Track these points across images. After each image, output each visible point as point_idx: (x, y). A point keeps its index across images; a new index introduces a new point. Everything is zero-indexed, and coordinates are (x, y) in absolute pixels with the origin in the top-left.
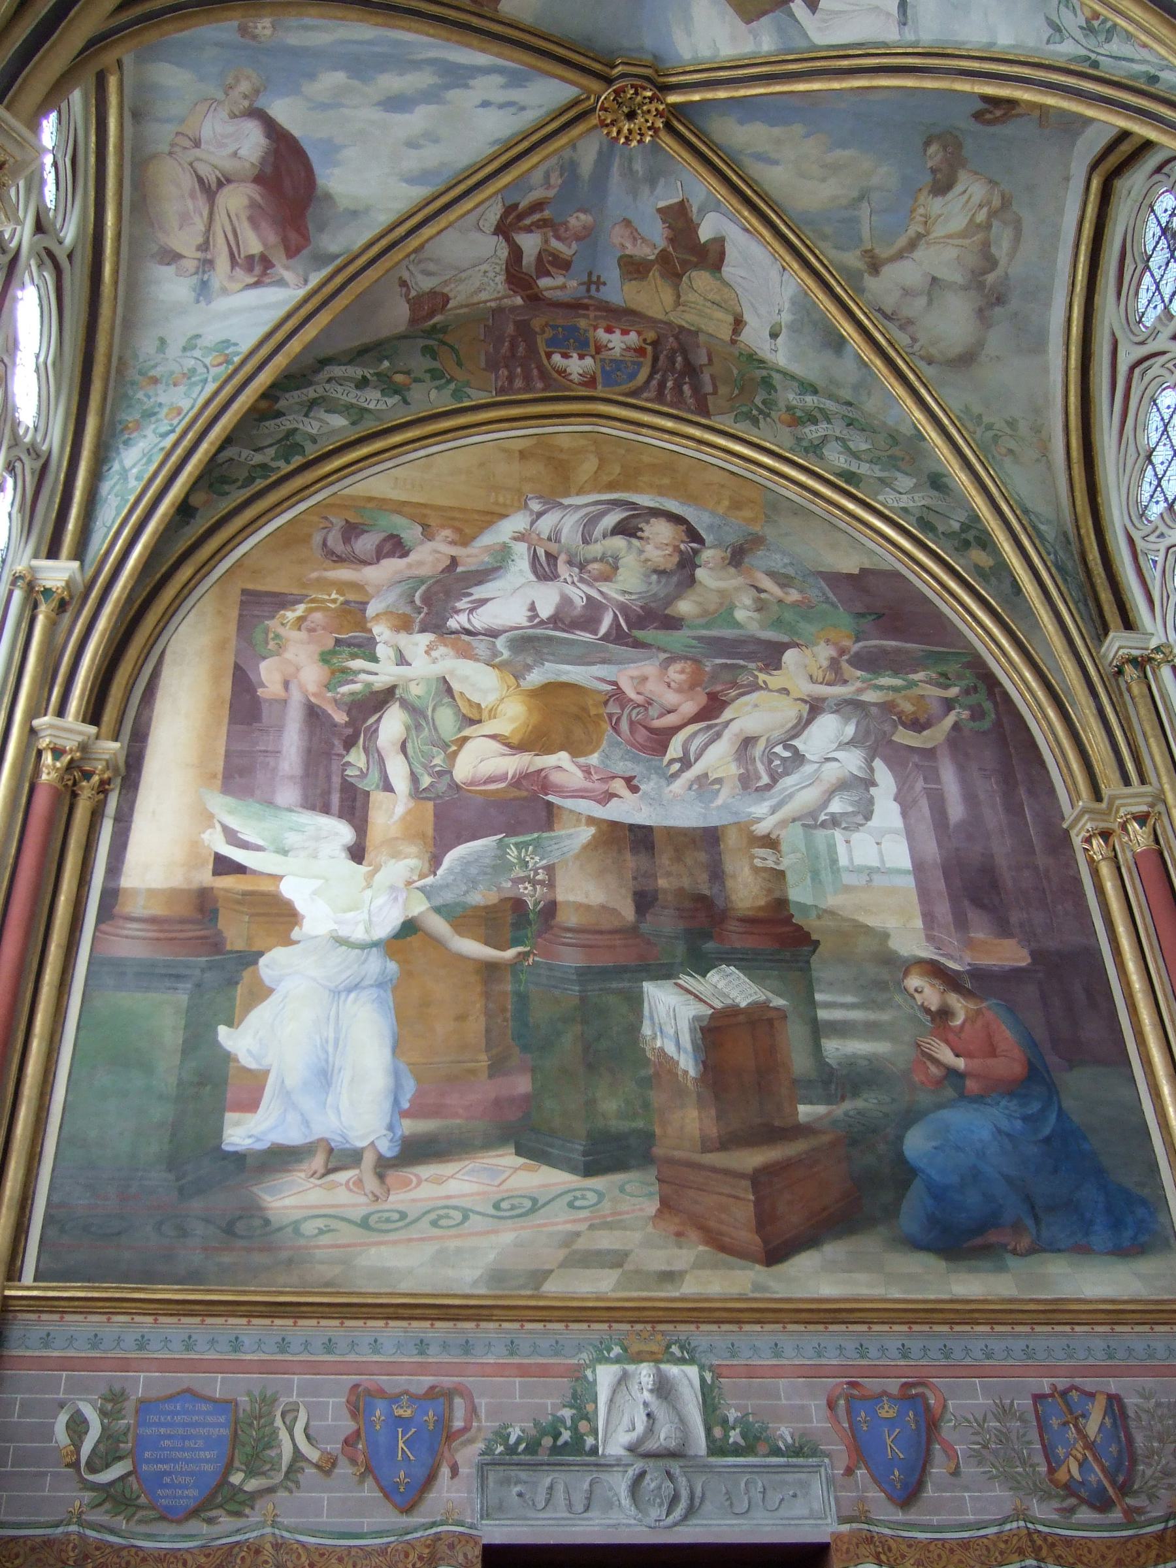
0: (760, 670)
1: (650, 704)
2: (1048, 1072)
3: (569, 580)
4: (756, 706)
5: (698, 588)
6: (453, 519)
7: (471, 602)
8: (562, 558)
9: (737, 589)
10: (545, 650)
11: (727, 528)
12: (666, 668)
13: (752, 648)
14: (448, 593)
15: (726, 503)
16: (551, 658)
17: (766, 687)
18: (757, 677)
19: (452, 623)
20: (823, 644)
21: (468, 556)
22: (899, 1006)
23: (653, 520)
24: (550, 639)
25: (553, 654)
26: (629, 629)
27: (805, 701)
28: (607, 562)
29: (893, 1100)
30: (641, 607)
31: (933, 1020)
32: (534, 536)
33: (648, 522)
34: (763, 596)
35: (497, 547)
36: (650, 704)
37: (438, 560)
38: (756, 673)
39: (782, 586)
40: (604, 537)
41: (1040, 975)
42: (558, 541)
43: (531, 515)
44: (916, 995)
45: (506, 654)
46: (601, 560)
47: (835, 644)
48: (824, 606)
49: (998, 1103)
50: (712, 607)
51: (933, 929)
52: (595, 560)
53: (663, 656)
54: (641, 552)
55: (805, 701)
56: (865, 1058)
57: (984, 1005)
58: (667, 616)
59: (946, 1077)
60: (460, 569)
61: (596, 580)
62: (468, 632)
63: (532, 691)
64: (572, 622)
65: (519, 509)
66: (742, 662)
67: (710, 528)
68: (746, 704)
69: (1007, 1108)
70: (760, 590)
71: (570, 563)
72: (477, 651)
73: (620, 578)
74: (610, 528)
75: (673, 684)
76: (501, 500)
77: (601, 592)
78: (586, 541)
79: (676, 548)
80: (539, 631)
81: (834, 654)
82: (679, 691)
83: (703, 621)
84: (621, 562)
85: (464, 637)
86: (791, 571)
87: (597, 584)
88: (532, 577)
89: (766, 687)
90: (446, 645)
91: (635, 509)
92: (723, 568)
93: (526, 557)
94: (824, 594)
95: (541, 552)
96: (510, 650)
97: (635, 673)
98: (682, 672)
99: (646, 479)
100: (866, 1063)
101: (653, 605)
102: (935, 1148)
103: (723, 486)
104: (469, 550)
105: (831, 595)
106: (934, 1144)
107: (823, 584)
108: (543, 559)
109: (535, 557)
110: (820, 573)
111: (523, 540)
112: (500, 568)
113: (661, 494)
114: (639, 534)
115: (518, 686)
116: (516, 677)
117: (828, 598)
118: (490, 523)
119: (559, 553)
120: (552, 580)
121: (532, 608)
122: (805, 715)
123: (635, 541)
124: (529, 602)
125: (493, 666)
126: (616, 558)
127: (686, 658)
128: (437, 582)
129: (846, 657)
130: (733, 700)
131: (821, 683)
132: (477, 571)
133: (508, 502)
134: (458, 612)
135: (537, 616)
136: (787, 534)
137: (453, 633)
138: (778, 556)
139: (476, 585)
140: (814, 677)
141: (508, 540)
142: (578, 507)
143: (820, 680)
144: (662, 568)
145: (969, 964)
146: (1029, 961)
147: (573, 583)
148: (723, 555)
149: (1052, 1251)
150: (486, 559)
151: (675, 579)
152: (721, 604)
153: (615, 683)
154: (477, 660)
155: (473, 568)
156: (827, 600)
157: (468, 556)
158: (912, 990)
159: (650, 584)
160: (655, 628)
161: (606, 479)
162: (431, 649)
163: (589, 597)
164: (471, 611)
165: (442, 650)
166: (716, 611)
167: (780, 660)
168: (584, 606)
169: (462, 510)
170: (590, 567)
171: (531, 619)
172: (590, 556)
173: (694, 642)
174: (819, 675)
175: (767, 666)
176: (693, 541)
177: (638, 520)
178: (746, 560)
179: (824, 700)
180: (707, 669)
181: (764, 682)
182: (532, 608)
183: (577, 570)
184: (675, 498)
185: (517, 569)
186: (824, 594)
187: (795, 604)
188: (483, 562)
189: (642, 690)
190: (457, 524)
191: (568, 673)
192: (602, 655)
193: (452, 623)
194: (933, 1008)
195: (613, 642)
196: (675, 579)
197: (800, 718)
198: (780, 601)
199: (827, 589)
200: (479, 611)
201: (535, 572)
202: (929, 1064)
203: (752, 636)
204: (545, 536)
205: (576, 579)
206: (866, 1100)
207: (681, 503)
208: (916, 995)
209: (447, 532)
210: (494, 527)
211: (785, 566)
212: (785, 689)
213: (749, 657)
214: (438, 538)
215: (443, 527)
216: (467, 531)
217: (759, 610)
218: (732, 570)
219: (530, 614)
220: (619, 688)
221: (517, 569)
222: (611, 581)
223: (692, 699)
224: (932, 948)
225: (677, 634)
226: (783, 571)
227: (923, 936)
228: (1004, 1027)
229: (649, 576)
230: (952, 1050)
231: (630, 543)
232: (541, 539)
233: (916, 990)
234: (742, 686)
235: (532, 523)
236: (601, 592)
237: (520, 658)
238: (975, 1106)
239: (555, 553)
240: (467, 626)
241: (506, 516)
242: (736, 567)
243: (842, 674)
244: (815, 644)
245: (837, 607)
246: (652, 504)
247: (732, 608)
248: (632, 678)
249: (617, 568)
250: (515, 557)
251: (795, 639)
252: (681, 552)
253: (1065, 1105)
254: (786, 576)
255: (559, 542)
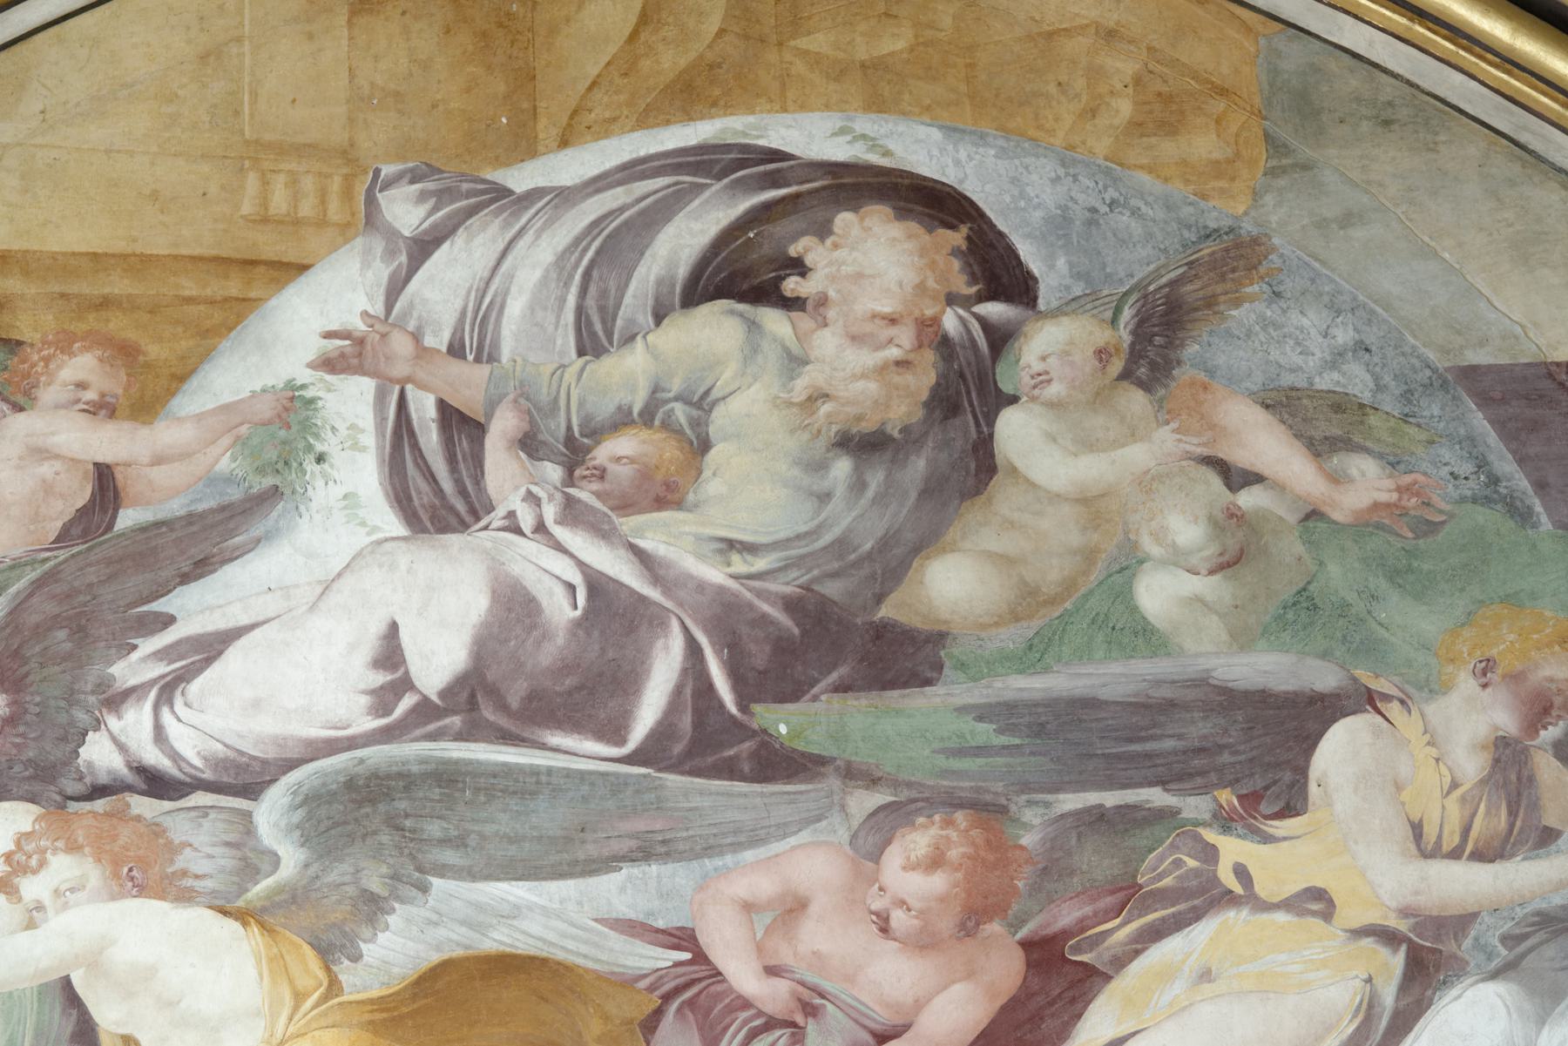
0: (1225, 821)
1: (810, 1010)
3: (526, 520)
4: (1206, 976)
5: (1004, 498)
6: (105, 303)
7: (162, 655)
8: (503, 426)
9: (1147, 482)
10: (434, 829)
11: (1123, 219)
12: (876, 856)
13: (1200, 729)
14: (81, 630)
15: (1124, 108)
16: (450, 856)
17: (1246, 896)
18: (1210, 854)
19: (99, 755)
20: (1466, 683)
21: (158, 460)
23: (844, 220)
24: (448, 777)
25: (459, 842)
26: (744, 708)
27: (1389, 937)
28: (666, 426)
30: (791, 605)
32: (401, 344)
33: (823, 231)
34: (1248, 499)
35: (266, 409)
36: (810, 1010)
37: (47, 488)
38: (1210, 836)
39: (1319, 448)
40: (659, 318)
42: (486, 354)
43: (390, 253)
45: (292, 859)
46: (647, 417)
47: (1515, 678)
48: (1483, 516)
50: (1052, 573)
52: (622, 421)
53: (864, 802)
54: (795, 362)
55: (1389, 937)
58: (883, 631)
60: (127, 519)
61: (626, 506)
62: (156, 784)
63: (380, 1003)
64: (532, 696)
65: (346, 232)
66: (1156, 797)
67: (1058, 227)
68: (1167, 974)
70: (1235, 477)
71: (529, 444)
72: (186, 860)
73: (712, 487)
74: (682, 272)
75: (899, 919)
76: (279, 201)
77: (643, 558)
78: (590, 344)
79: (928, 329)
80: (411, 750)
81: (1502, 717)
82: (923, 943)
83: (1011, 637)
84: (719, 420)
85: (143, 806)
86: (1356, 380)
87: (627, 524)
88: (393, 525)
89: (1246, 896)
90: (73, 848)
91: (773, 180)
92: (1100, 399)
93: (369, 440)
94: (1482, 464)
95: (424, 408)
96: (305, 842)
97: (763, 885)
98: (935, 862)
99: (818, 42)
101: (832, 589)
103: (1110, 35)
104: (166, 434)
105: (1505, 465)
107: (1479, 421)
108: (430, 438)
109: (403, 430)
110: (1469, 375)
111: (360, 370)
112: (273, 495)
113: (877, 104)
114: (792, 285)
115: (334, 986)
116: (326, 953)
117: (1494, 480)
118: (237, 311)
119: (491, 407)
120: (463, 526)
121: (390, 653)
122: (1388, 995)
123: (774, 320)
124: (377, 627)
125: (243, 916)
126: (703, 403)
127: (954, 802)
128: (39, 584)
129: (1550, 734)
130: (1121, 962)
131: (1455, 854)
132: (190, 519)
133: (307, 209)
134: (116, 700)
135: (405, 684)
136: (1348, 219)
137: (99, 791)
138: (1310, 321)
139: (185, 579)
140: (1430, 832)
141: (305, 375)
142: (565, 197)
143: (1451, 840)
144: (868, 426)
147: (540, 528)
148: (1103, 336)
150: (225, 464)
151: (918, 466)
152: (1089, 556)
153: (683, 938)
154: (185, 897)
155: (175, 507)
156: (1492, 492)
157: (158, 460)
159: (824, 497)
160: (842, 688)
161: (669, 61)
162: (24, 870)
163: (598, 585)
164: (168, 689)
165: (62, 867)
166: (1069, 586)
167: (1302, 771)
168: (578, 624)
169: (138, 264)
170: (604, 453)
171: (383, 699)
172: (605, 409)
173: (985, 732)
174: (1444, 817)
175: (1251, 800)
176: (993, 293)
177: (779, 229)
178: (1192, 349)
179: (1464, 921)
180: (1028, 840)
181: (1241, 872)
182: (390, 653)
183: (554, 472)
184: (927, 111)
185: (337, 491)
186: (1482, 464)
187: (1370, 522)
188: (213, 480)
189: (785, 956)
190: (118, 325)
191: (515, 912)
192: (640, 825)
193: (99, 755)
195: (676, 767)
196: (918, 466)
197: (1370, 1008)
198: (1313, 514)
199: (1493, 438)
200: (195, 687)
201: (402, 500)
203: (1202, 682)
204: (438, 340)
205: (550, 512)
207: (950, 130)
209: (81, 366)
210: (255, 326)
211: (1336, 359)
212: (1319, 894)
213: (1172, 777)
214: (49, 394)
215: (65, 344)
216: (154, 351)
217: (1226, 565)
218: (1135, 401)
219: (380, 678)
220: (700, 957)
221: (337, 491)
222: (679, 505)
223: (970, 975)
225: (918, 701)
226: (1325, 382)
229: (819, 467)
231: (753, 326)
232: (422, 352)
234: (1163, 897)
235: (395, 289)
236: (643, 558)
237: (339, 872)
239: (474, 409)
240: (153, 757)
241: (303, 268)
242: (1146, 386)
243: (1535, 806)
244: (1435, 688)
245: (1523, 516)
246: (839, 151)
247: (1129, 563)
248: (748, 908)
249: (705, 446)
250: (328, 444)
251: (1365, 676)
252: (945, 344)
254: (1339, 404)
255: (492, 359)
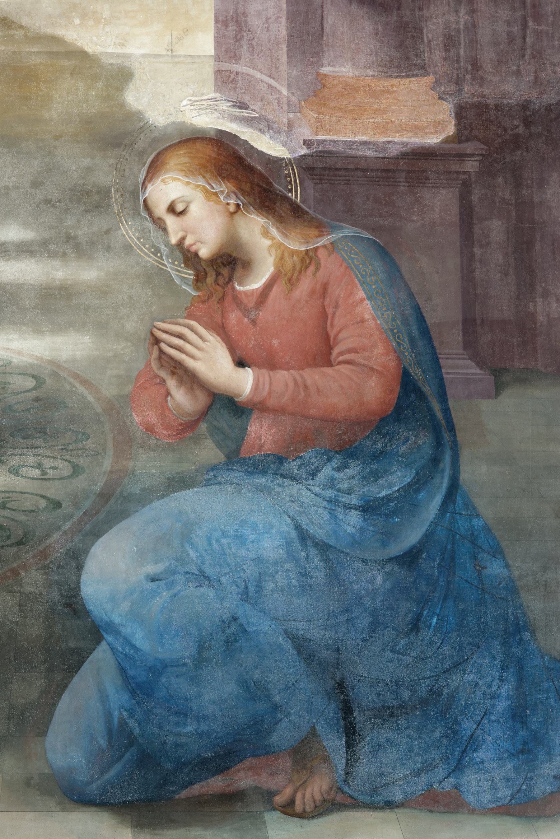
2: (443, 397)
22: (128, 248)
29: (77, 470)
31: (199, 279)
41: (471, 166)
44: (170, 221)
49: (313, 474)
51: (236, 57)
56: (23, 372)
57: (324, 241)
59: (204, 414)
69: (332, 483)
100: (30, 383)
102: (153, 579)
106: (151, 569)
145: (307, 143)
146: (451, 130)
149: (374, 807)
158: (160, 210)
194: (204, 252)
202: (171, 383)
206: (14, 471)
208: (170, 221)
224: (225, 106)
227: (209, 70)
228: (361, 294)
230: (232, 348)
233: (171, 209)
238: (261, 481)
253: (465, 475)
